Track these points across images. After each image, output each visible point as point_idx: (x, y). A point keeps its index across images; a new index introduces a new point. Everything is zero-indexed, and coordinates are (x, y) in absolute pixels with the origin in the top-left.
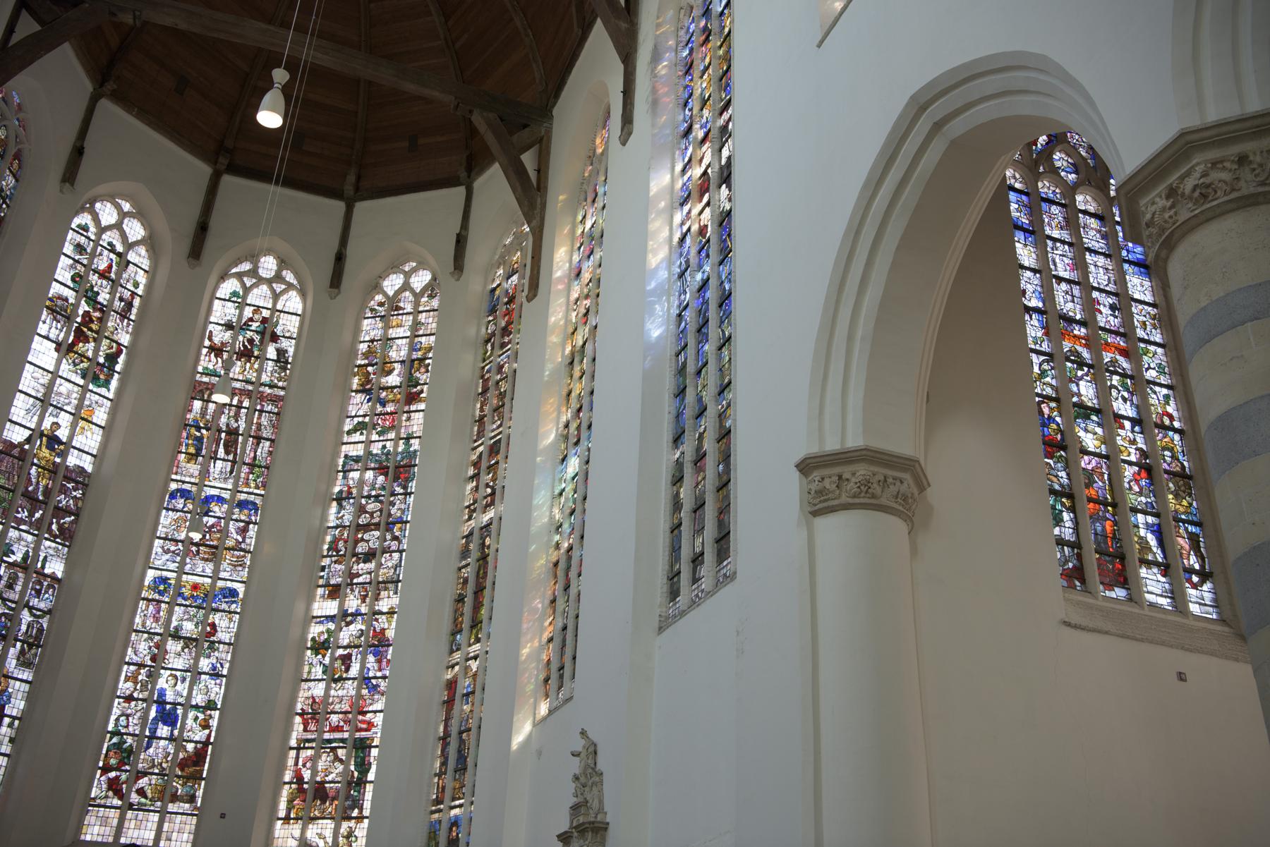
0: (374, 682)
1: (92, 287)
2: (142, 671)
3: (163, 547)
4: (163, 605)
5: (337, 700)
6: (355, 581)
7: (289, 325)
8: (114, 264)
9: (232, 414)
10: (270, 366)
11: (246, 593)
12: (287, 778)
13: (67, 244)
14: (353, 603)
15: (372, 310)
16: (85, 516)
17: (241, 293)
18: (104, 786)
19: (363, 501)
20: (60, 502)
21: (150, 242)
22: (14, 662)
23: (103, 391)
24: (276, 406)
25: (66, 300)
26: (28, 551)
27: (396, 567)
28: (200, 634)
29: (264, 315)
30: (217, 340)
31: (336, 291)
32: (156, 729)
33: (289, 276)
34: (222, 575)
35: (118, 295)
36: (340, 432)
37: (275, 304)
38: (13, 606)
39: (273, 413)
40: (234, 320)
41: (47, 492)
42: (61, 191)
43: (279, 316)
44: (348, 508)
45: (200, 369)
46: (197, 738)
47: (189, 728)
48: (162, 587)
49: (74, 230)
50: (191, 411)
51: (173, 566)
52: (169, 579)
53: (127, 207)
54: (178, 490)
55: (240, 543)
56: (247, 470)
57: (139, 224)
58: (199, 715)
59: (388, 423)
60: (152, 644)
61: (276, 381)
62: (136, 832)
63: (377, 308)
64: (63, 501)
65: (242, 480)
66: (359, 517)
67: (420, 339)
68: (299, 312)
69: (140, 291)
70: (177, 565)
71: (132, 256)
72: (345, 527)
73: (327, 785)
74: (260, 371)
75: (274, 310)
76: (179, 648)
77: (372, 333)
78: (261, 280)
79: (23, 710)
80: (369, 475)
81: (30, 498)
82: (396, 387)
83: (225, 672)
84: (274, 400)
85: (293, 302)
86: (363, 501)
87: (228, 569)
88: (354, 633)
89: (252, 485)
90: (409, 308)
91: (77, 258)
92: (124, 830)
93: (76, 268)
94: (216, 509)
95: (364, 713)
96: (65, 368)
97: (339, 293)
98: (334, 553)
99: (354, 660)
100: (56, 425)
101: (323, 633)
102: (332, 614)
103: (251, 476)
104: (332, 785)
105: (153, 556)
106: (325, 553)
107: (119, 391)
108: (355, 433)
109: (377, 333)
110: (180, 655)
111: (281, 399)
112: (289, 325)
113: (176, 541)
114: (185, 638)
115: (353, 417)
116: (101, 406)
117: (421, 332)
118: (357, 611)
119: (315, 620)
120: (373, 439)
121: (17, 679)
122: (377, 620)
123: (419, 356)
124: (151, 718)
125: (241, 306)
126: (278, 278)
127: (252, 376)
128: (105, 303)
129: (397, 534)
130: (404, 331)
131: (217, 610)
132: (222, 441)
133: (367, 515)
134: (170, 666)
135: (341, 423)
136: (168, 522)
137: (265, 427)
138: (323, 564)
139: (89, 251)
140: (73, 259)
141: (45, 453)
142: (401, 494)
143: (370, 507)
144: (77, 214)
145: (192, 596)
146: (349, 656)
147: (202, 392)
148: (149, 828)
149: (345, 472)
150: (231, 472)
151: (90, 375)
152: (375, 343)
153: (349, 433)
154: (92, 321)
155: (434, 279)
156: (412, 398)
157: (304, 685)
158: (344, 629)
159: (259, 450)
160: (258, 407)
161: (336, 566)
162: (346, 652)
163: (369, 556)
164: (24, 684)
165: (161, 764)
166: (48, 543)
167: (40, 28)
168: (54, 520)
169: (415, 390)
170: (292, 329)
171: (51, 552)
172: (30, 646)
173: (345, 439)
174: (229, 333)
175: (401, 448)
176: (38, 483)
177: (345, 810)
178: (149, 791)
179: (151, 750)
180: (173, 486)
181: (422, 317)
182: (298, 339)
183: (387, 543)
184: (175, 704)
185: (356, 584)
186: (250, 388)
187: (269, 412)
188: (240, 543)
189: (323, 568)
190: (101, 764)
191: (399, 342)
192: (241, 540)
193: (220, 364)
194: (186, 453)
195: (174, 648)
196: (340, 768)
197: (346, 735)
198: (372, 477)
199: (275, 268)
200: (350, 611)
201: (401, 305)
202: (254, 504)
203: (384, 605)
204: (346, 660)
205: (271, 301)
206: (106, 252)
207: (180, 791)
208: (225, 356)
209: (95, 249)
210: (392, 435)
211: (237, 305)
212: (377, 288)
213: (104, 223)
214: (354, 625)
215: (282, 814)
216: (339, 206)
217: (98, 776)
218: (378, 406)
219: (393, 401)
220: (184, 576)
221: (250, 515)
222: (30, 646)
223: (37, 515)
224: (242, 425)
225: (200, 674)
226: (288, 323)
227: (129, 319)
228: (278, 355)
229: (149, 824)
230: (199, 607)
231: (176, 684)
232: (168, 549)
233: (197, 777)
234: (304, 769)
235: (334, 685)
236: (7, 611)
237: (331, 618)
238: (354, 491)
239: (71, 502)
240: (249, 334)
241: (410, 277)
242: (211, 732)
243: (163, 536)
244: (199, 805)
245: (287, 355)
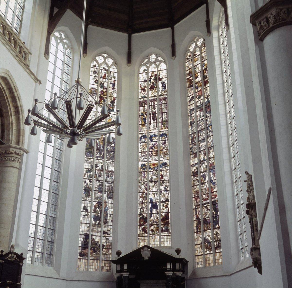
0: (214, 181)
1: (101, 82)
2: (144, 194)
3: (141, 155)
4: (146, 173)
5: (204, 190)
6: (201, 150)
7: (163, 74)
8: (106, 74)
9: (152, 108)
10: (160, 89)
11: (169, 163)
12: (195, 219)
13: (91, 72)
14: (202, 157)
15: (188, 59)
17: (147, 69)
18: (141, 230)
19: (198, 123)
20: (108, 149)
21: (115, 63)
22: (106, 198)
24: (166, 101)
25: (95, 89)
26: (102, 165)
27: (212, 141)
28: (158, 179)
29: (155, 73)
30: (143, 87)
31: (174, 57)
32: (152, 211)
33: (160, 59)
34: (161, 159)
35: (110, 83)
36: (186, 103)
37: (158, 69)
38: (102, 182)
39: (165, 104)
40: (146, 78)
42: (84, 57)
43: (160, 72)
44: (194, 126)
45: (140, 97)
46: (165, 211)
47: (162, 208)
48: (144, 167)
49: (92, 68)
50: (140, 111)
51: (145, 160)
52: (146, 164)
53: (105, 55)
54: (142, 136)
55: (164, 147)
56: (161, 124)
57: (111, 59)
58: (164, 204)
59: (200, 94)
60: (145, 185)
61: (163, 93)
62: (154, 243)
63: (189, 57)
65: (160, 127)
66: (198, 128)
67: (204, 62)
68: (166, 69)
69: (116, 79)
70: (147, 159)
71: (111, 70)
72: (195, 133)
73: (207, 219)
74: (158, 92)
75: (158, 71)
76: (153, 184)
77: (189, 67)
78: (151, 63)
79: (113, 212)
80: (198, 113)
82: (200, 81)
83: (169, 189)
84: (165, 99)
85: (163, 66)
86: (198, 123)
87: (162, 157)
88: (204, 167)
89: (164, 128)
90: (198, 53)
91: (95, 75)
92: (150, 243)
93: (95, 78)
94: (154, 139)
95: (213, 193)
97: (175, 56)
98: (193, 143)
99: (206, 176)
101: (195, 169)
102: (196, 162)
103: (163, 125)
104: (208, 218)
105: (139, 158)
106: (191, 144)
108: (191, 101)
109: (190, 66)
110: (154, 187)
111: (166, 98)
112: (163, 74)
113: (145, 152)
114: (154, 181)
115: (189, 96)
117: (204, 60)
118: (204, 159)
119: (192, 166)
120: (197, 101)
121: (108, 203)
122: (210, 160)
123: (205, 68)
124: (150, 208)
125: (147, 74)
126: (157, 60)
127: (156, 94)
128: (107, 86)
129: (211, 130)
130: (199, 61)
131: (161, 171)
132: (151, 117)
133: (200, 127)
134: (152, 191)
135: (186, 99)
136: (141, 147)
137: (164, 109)
138: (191, 147)
139: (98, 72)
140: (94, 76)
142: (209, 116)
143: (201, 124)
144: (91, 62)
145: (153, 168)
146: (205, 174)
147: (142, 104)
148: (157, 241)
149: (191, 115)
150: (156, 126)
152: (191, 69)
153: (189, 102)
154: (104, 93)
155: (204, 40)
156: (206, 83)
157: (194, 188)
158: (201, 166)
159: (163, 117)
160: (160, 103)
161: (195, 146)
162: (203, 174)
163: (204, 140)
164: (111, 204)
165: (156, 221)
166: (107, 162)
167: (58, 9)
168: (108, 154)
169: (206, 80)
170: (165, 75)
171: (109, 164)
172: (110, 193)
173: (189, 104)
174: (146, 83)
175: (206, 101)
176: (100, 145)
177: (214, 226)
178: (155, 230)
179: (152, 217)
180: (140, 135)
181: (203, 55)
182: (167, 78)
183: (208, 134)
184: (156, 202)
185: (202, 151)
186: (156, 98)
187: (164, 104)
188: (164, 147)
189: (191, 149)
190: (139, 224)
191: (198, 66)
192: (164, 146)
193: (145, 94)
194: (141, 124)
195: (152, 185)
196: (209, 212)
197: (209, 201)
198: (199, 114)
199: (155, 57)
200: (202, 160)
201: (196, 53)
202: (166, 134)
203: (211, 155)
204: (204, 177)
205: (156, 68)
206: (103, 71)
207: (163, 228)
208: (146, 90)
209: (99, 71)
210: (202, 98)
211: (146, 73)
212: (187, 50)
214: (204, 164)
215: (196, 231)
216: (169, 29)
217: (139, 228)
218: (196, 89)
219: (200, 86)
220: (150, 162)
221: (165, 138)
222: (110, 193)
223: (102, 154)
224: (156, 110)
225: (161, 191)
226: (163, 73)
227: (115, 89)
228: (162, 85)
229: (157, 240)
230: (156, 171)
231: (155, 196)
232: (143, 155)
233: (168, 223)
234: (199, 215)
235: (202, 185)
236: (101, 184)
237: (196, 164)
238: (195, 120)
239: (111, 148)
240: (152, 81)
241: (197, 43)
242: (169, 209)
243: (141, 151)
244: (170, 232)
245: (165, 84)
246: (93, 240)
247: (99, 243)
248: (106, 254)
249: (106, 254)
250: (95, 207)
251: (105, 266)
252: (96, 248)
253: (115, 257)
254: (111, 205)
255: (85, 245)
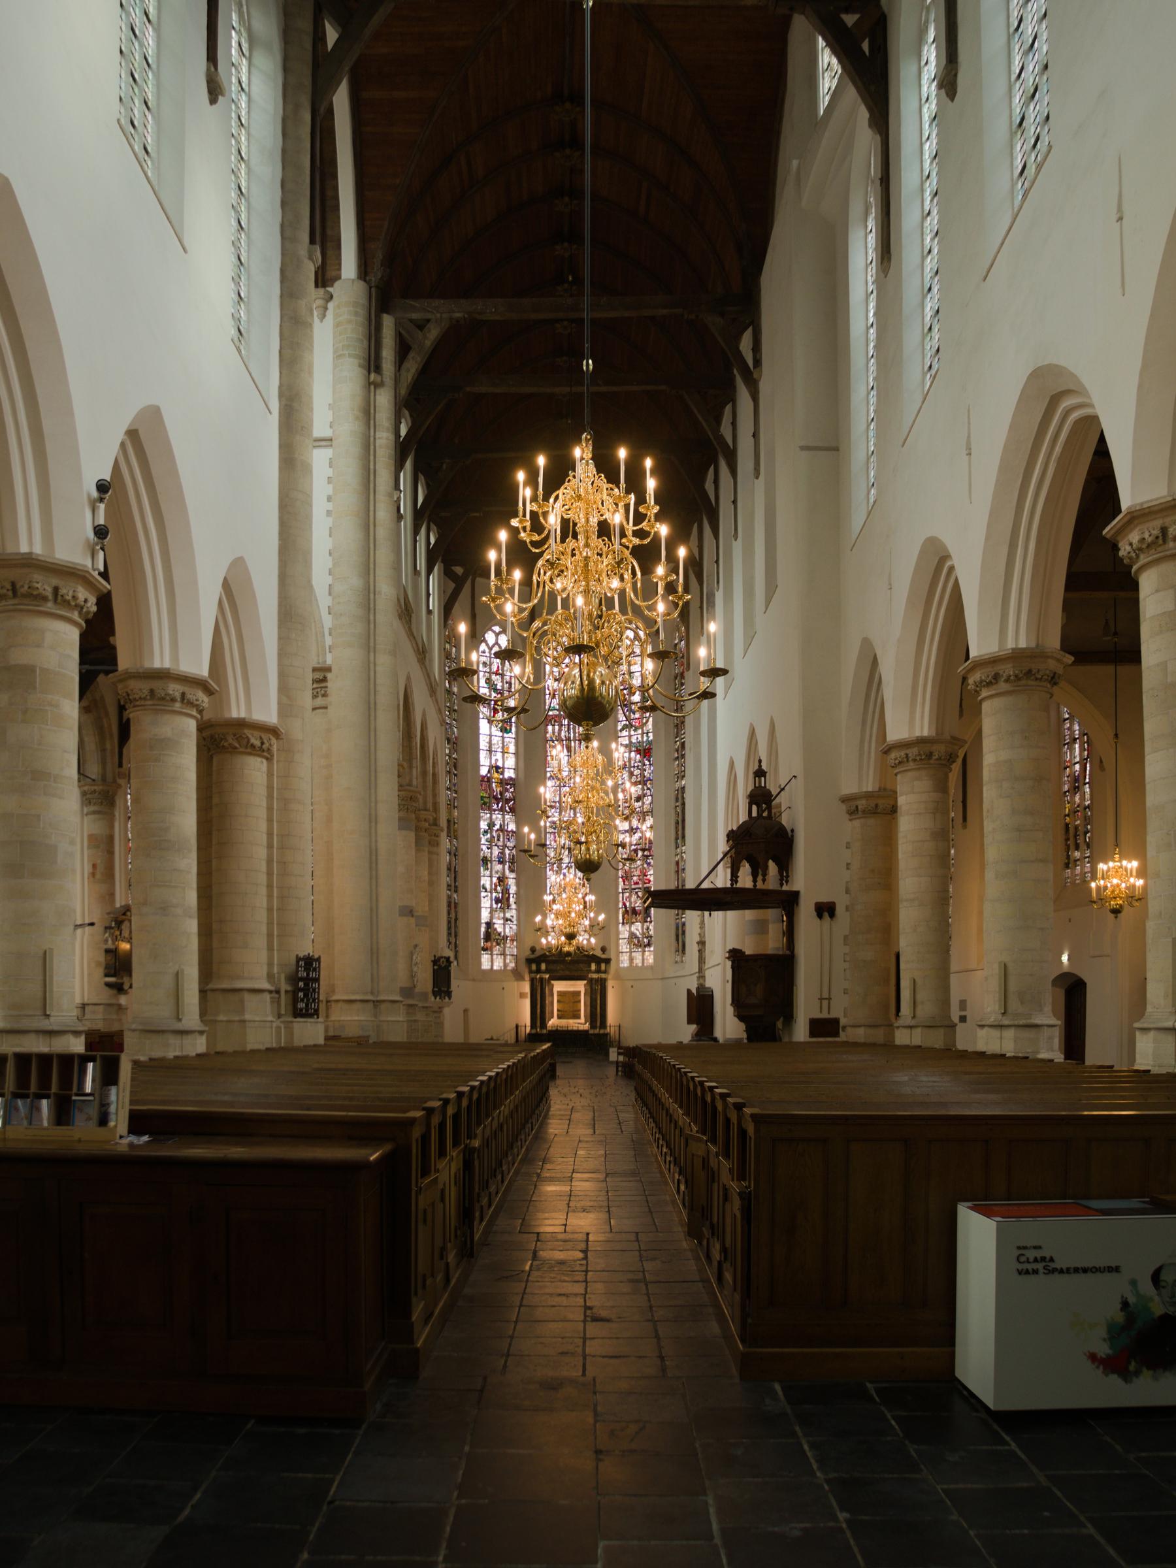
16: (517, 799)
23: (510, 735)
41: (501, 793)
64: (508, 795)
81: (495, 798)
96: (496, 732)
100: (497, 760)
107: (517, 733)
116: (511, 743)
141: (496, 775)
151: (503, 730)
213: (491, 645)
223: (500, 805)
246: (495, 929)
247: (502, 934)
248: (510, 947)
249: (510, 947)
250: (496, 886)
251: (511, 962)
252: (502, 940)
253: (528, 953)
254: (514, 881)
255: (488, 937)
